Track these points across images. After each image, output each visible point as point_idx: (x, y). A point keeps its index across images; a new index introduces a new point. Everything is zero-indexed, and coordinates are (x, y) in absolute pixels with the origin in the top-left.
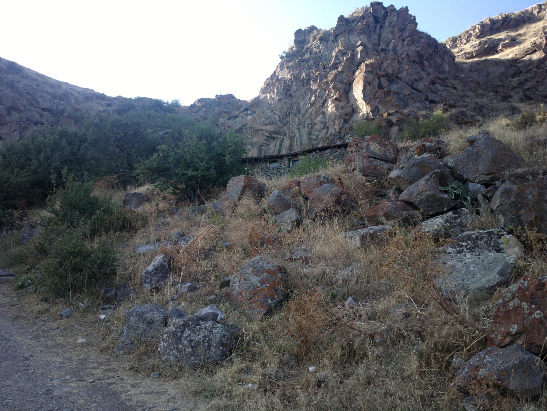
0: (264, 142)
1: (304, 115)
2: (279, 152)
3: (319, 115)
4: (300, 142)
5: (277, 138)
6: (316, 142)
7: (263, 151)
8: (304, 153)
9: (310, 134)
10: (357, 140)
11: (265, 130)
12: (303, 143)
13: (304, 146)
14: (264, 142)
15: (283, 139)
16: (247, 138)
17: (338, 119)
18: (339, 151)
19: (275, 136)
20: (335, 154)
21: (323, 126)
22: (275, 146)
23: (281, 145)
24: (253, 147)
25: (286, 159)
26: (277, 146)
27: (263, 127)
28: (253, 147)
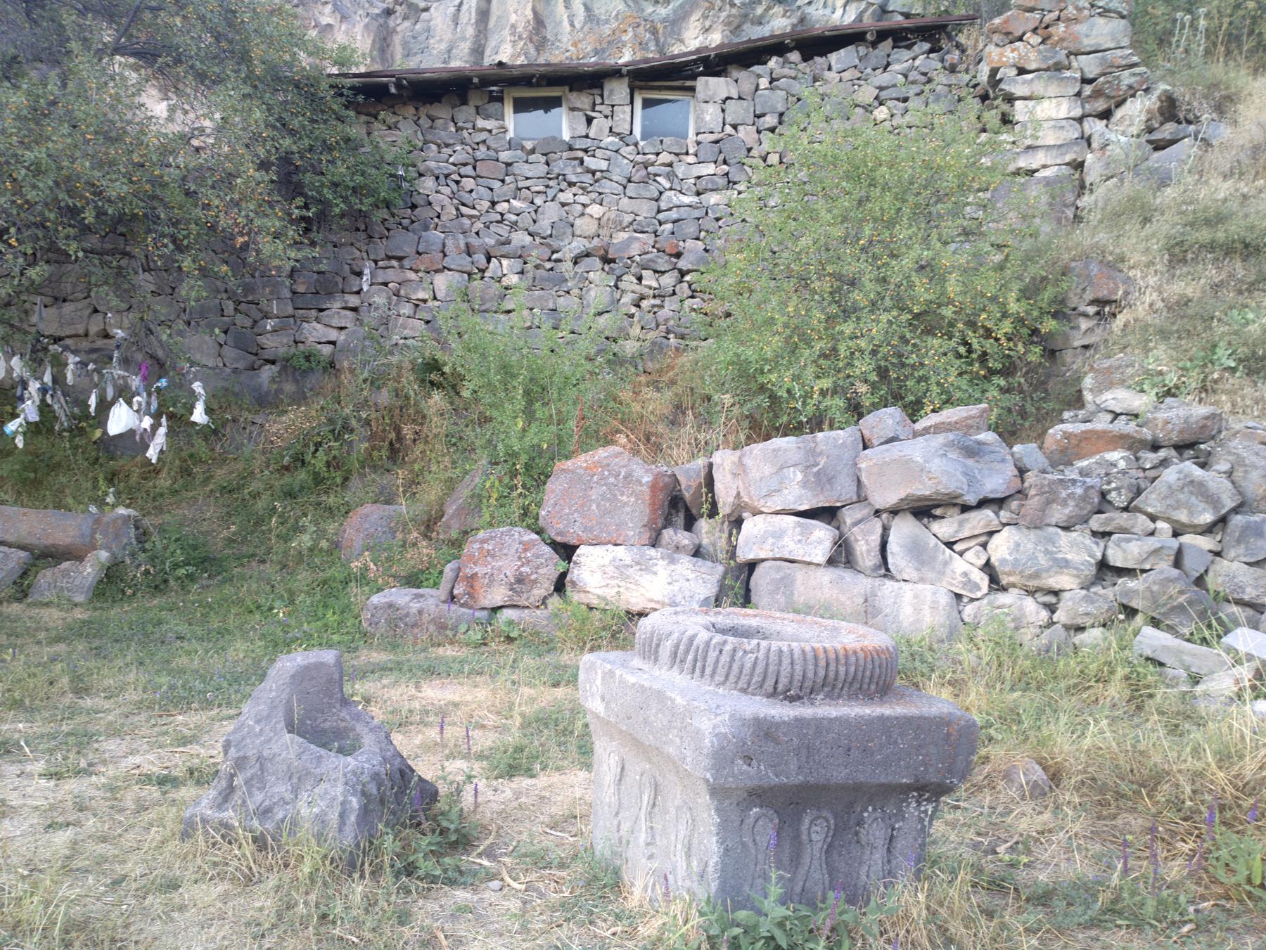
2: (478, 51)
4: (587, 8)
7: (397, 39)
8: (717, 64)
12: (599, 10)
13: (607, 30)
18: (902, 60)
20: (883, 78)
23: (483, 15)
24: (344, 18)
25: (618, 91)
28: (344, 18)
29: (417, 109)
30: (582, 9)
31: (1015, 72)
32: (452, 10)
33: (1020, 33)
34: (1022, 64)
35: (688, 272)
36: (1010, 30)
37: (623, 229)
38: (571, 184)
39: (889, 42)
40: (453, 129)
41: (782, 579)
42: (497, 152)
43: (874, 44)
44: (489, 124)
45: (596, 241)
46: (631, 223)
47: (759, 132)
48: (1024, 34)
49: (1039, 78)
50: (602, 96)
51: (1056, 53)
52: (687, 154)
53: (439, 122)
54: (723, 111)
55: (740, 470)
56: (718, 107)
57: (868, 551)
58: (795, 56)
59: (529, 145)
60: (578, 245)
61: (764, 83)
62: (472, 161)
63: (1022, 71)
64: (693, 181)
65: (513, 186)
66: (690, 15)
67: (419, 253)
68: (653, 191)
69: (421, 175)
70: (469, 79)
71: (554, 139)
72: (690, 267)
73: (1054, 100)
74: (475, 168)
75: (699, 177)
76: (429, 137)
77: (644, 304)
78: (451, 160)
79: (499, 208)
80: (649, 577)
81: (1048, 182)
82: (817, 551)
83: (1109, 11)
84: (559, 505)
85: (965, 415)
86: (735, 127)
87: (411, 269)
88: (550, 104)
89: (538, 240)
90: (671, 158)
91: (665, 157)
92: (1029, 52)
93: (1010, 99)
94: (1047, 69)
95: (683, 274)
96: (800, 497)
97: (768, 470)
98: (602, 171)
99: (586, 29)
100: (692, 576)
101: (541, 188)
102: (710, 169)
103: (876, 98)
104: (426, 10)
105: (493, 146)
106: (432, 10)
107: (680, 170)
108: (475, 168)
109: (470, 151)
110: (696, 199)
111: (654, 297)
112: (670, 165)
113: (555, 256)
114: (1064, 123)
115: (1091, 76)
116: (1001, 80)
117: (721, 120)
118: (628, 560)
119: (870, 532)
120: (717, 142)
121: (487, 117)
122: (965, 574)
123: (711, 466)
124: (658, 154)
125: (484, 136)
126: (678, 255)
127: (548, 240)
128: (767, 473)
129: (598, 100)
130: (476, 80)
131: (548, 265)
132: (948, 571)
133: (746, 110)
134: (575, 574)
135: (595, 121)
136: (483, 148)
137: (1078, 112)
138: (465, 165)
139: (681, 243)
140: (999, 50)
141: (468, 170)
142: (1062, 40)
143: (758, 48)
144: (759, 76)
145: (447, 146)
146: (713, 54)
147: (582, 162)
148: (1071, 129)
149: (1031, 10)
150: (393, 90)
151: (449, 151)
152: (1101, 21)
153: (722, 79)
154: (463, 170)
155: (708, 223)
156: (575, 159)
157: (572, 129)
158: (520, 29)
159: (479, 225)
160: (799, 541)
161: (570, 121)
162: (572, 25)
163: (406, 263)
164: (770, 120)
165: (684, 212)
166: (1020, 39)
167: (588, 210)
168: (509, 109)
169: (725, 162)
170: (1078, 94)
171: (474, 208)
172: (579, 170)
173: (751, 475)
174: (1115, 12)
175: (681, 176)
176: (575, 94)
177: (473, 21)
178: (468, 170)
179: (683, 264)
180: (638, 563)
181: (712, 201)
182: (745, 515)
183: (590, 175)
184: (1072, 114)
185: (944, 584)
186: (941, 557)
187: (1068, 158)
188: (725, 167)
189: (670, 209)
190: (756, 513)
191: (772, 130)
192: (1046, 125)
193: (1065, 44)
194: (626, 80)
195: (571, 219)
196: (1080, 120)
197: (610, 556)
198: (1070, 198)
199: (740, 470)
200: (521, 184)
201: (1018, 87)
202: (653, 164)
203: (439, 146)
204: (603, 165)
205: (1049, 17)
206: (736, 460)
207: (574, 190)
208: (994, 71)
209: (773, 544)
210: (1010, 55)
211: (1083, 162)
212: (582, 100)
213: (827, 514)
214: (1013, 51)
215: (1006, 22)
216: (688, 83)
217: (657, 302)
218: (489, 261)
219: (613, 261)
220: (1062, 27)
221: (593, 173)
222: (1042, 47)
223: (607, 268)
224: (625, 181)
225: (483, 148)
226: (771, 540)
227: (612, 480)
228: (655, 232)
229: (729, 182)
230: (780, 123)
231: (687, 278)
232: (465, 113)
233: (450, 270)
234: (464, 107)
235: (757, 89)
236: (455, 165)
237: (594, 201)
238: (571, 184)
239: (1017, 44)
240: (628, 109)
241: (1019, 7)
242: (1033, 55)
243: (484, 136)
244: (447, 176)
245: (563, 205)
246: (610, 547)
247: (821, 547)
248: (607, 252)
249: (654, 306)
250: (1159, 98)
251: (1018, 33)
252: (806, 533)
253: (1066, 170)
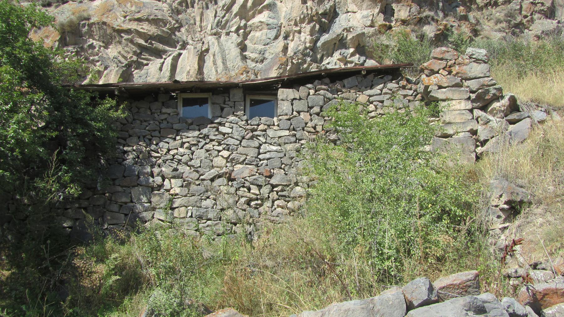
0: (135, 58)
1: (228, 9)
3: (260, 12)
5: (165, 52)
6: (259, 66)
9: (243, 48)
10: (447, 56)
11: (137, 32)
12: (229, 65)
13: (233, 73)
14: (135, 58)
15: (180, 54)
16: (92, 47)
17: (309, 23)
19: (161, 46)
21: (273, 33)
22: (161, 69)
26: (164, 68)
27: (133, 26)
29: (131, 103)
30: (221, 64)
31: (437, 88)
32: (159, 65)
33: (437, 70)
34: (440, 84)
35: (277, 186)
36: (433, 68)
37: (240, 163)
38: (212, 140)
39: (372, 75)
40: (149, 113)
42: (172, 124)
43: (365, 76)
44: (169, 111)
45: (224, 170)
46: (244, 160)
47: (311, 115)
48: (439, 70)
49: (449, 90)
50: (229, 97)
51: (456, 79)
52: (274, 125)
53: (142, 110)
54: (292, 104)
56: (290, 104)
58: (327, 80)
59: (190, 121)
60: (214, 172)
61: (312, 92)
62: (158, 128)
63: (440, 87)
64: (277, 138)
65: (180, 141)
66: (273, 67)
67: (125, 177)
68: (256, 143)
69: (130, 136)
70: (159, 89)
71: (203, 117)
72: (277, 183)
73: (458, 101)
74: (160, 132)
75: (280, 137)
76: (136, 117)
77: (253, 203)
78: (147, 128)
79: (172, 152)
81: (459, 141)
83: (479, 60)
85: (465, 278)
86: (299, 112)
87: (119, 185)
88: (202, 102)
89: (193, 169)
90: (266, 127)
91: (261, 127)
92: (441, 78)
93: (437, 100)
94: (453, 86)
95: (273, 186)
98: (228, 134)
99: (223, 73)
101: (195, 142)
102: (287, 133)
103: (369, 101)
104: (147, 65)
105: (170, 121)
106: (150, 65)
107: (270, 133)
108: (160, 132)
109: (158, 124)
110: (279, 148)
111: (257, 199)
112: (265, 130)
113: (202, 177)
114: (464, 112)
115: (474, 90)
116: (430, 91)
117: (291, 109)
120: (289, 119)
121: (168, 107)
124: (258, 125)
125: (165, 116)
126: (270, 177)
127: (199, 169)
129: (227, 99)
130: (162, 89)
131: (197, 183)
133: (304, 105)
135: (225, 110)
136: (165, 122)
137: (469, 106)
138: (154, 131)
139: (272, 170)
140: (428, 78)
141: (157, 133)
142: (457, 73)
143: (309, 76)
144: (310, 89)
145: (145, 121)
146: (286, 78)
147: (218, 130)
148: (468, 114)
149: (442, 59)
150: (116, 93)
151: (146, 124)
152: (475, 64)
153: (291, 90)
154: (153, 134)
155: (285, 160)
156: (214, 127)
157: (213, 113)
158: (191, 73)
159: (160, 161)
161: (213, 109)
162: (217, 71)
163: (117, 182)
164: (316, 109)
165: (273, 155)
166: (438, 72)
167: (220, 154)
168: (180, 104)
169: (294, 130)
170: (469, 98)
171: (158, 153)
172: (217, 133)
174: (481, 60)
175: (271, 136)
176: (215, 96)
177: (169, 69)
178: (157, 133)
179: (273, 181)
181: (288, 148)
183: (222, 136)
184: (467, 108)
187: (468, 128)
188: (293, 132)
189: (265, 153)
191: (318, 114)
192: (454, 112)
193: (459, 75)
194: (242, 90)
195: (211, 158)
196: (471, 111)
198: (473, 148)
200: (184, 140)
201: (440, 94)
202: (256, 130)
203: (141, 121)
204: (229, 131)
205: (449, 64)
207: (214, 143)
208: (427, 87)
210: (434, 79)
211: (477, 130)
212: (219, 99)
214: (435, 78)
215: (430, 64)
216: (274, 92)
217: (259, 202)
218: (164, 181)
219: (234, 180)
220: (457, 67)
221: (224, 134)
222: (448, 76)
223: (230, 183)
224: (240, 138)
225: (165, 122)
228: (257, 165)
229: (296, 139)
230: (321, 111)
231: (275, 189)
232: (155, 106)
233: (141, 186)
234: (156, 103)
235: (309, 94)
236: (149, 131)
237: (224, 149)
238: (212, 140)
239: (437, 75)
240: (243, 103)
241: (435, 58)
242: (444, 80)
243: (165, 116)
244: (144, 137)
245: (207, 151)
248: (230, 174)
249: (256, 204)
250: (509, 99)
251: (436, 70)
253: (468, 134)
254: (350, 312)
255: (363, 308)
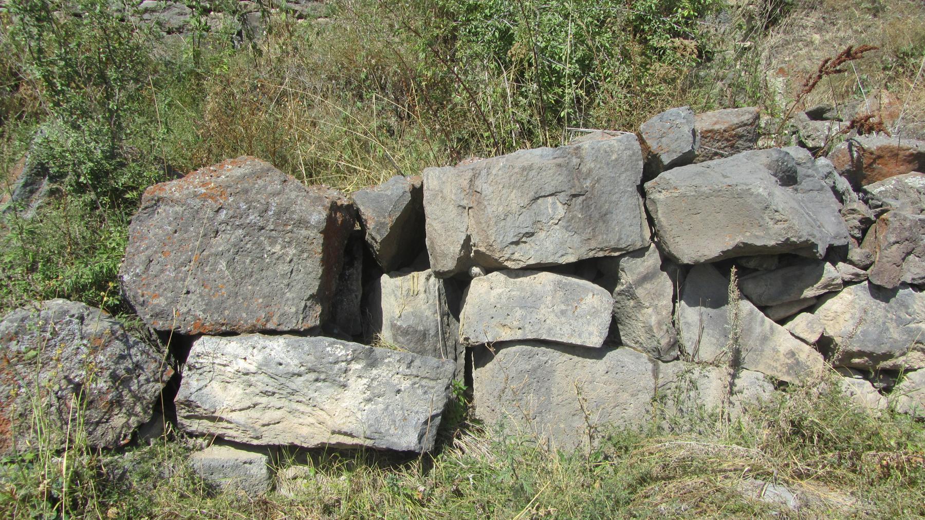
41: (534, 370)
55: (472, 200)
57: (660, 323)
80: (329, 390)
82: (591, 329)
84: (157, 256)
96: (563, 243)
97: (516, 200)
100: (405, 384)
118: (292, 363)
119: (659, 295)
122: (792, 354)
123: (417, 193)
128: (514, 207)
132: (768, 351)
134: (190, 385)
160: (563, 313)
173: (489, 210)
180: (311, 370)
182: (475, 270)
185: (761, 367)
186: (758, 330)
190: (491, 266)
197: (259, 357)
199: (472, 200)
206: (465, 184)
209: (523, 318)
213: (599, 270)
226: (519, 313)
227: (253, 218)
246: (258, 339)
247: (596, 322)
252: (572, 299)
254: (533, 173)
255: (560, 165)
